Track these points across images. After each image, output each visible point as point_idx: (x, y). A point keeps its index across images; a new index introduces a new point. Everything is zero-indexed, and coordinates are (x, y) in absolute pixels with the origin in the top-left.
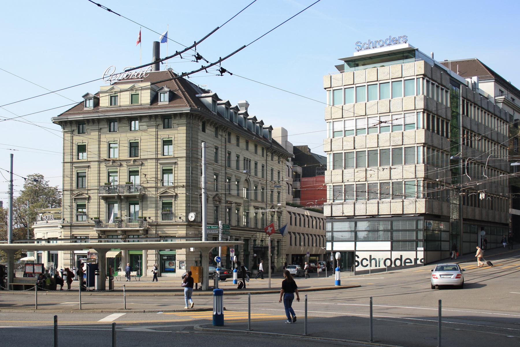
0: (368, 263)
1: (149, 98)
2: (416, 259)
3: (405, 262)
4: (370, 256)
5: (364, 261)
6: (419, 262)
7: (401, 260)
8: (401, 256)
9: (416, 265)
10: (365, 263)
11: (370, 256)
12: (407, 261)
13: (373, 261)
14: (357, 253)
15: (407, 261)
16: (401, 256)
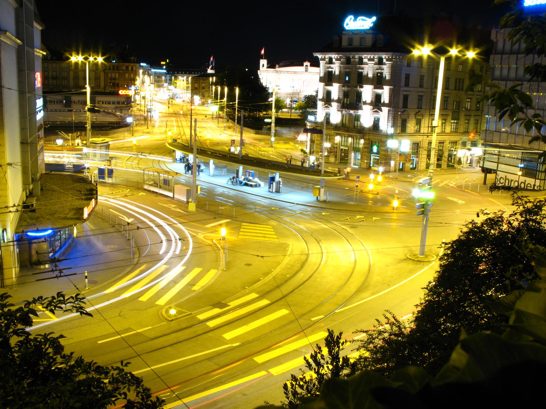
0: (504, 181)
1: (371, 42)
2: (534, 185)
3: (527, 186)
4: (506, 176)
5: (502, 179)
6: (536, 188)
7: (525, 184)
8: (525, 181)
9: (534, 190)
10: (502, 181)
11: (506, 176)
12: (529, 185)
13: (507, 181)
14: (498, 172)
15: (529, 185)
16: (525, 181)
